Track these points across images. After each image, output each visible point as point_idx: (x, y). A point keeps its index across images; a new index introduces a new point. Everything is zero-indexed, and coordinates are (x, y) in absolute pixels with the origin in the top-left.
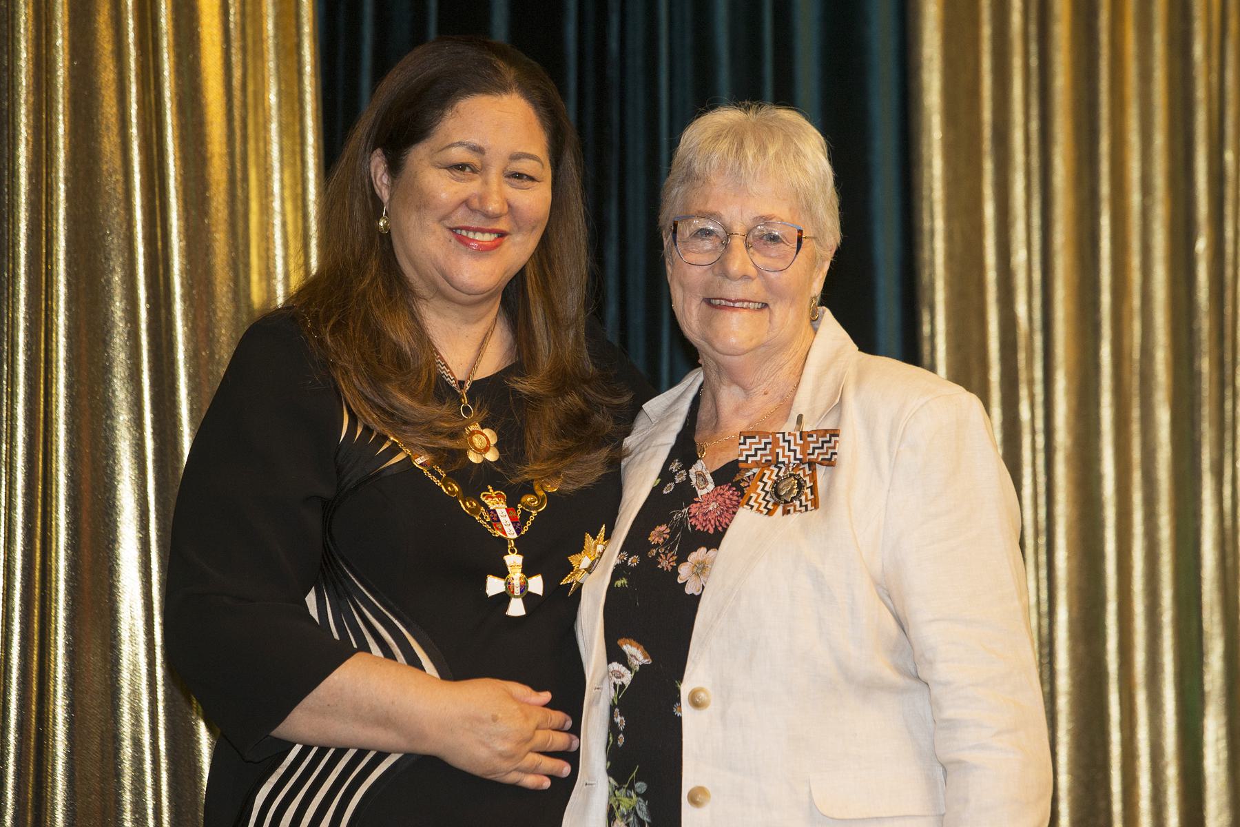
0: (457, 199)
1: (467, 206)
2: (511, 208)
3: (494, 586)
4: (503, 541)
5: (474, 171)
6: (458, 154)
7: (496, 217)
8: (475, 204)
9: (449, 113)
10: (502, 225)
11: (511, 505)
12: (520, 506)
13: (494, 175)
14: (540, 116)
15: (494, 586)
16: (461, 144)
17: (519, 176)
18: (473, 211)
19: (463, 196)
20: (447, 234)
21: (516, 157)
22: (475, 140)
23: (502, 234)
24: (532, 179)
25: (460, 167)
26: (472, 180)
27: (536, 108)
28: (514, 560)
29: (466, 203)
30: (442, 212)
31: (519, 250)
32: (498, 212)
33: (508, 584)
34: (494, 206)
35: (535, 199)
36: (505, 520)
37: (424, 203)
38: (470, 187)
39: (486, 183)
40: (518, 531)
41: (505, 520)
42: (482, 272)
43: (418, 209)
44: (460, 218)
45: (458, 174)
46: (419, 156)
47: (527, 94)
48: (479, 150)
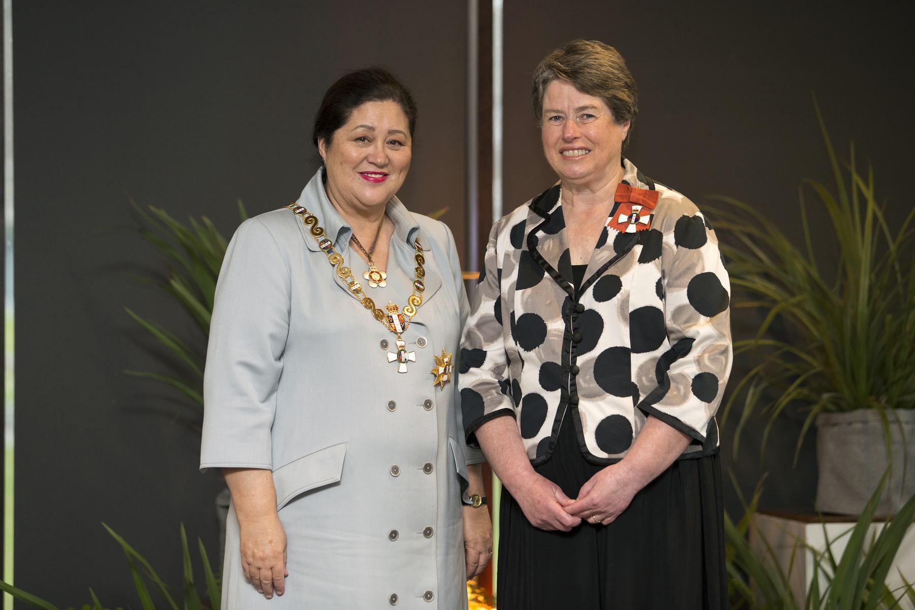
0: (362, 156)
6: (360, 132)
10: (385, 170)
13: (379, 143)
16: (362, 126)
17: (393, 142)
21: (391, 132)
22: (368, 123)
23: (385, 175)
24: (401, 144)
25: (362, 139)
26: (369, 146)
29: (366, 158)
34: (380, 160)
35: (402, 155)
38: (370, 150)
45: (360, 143)
46: (341, 135)
48: (372, 129)
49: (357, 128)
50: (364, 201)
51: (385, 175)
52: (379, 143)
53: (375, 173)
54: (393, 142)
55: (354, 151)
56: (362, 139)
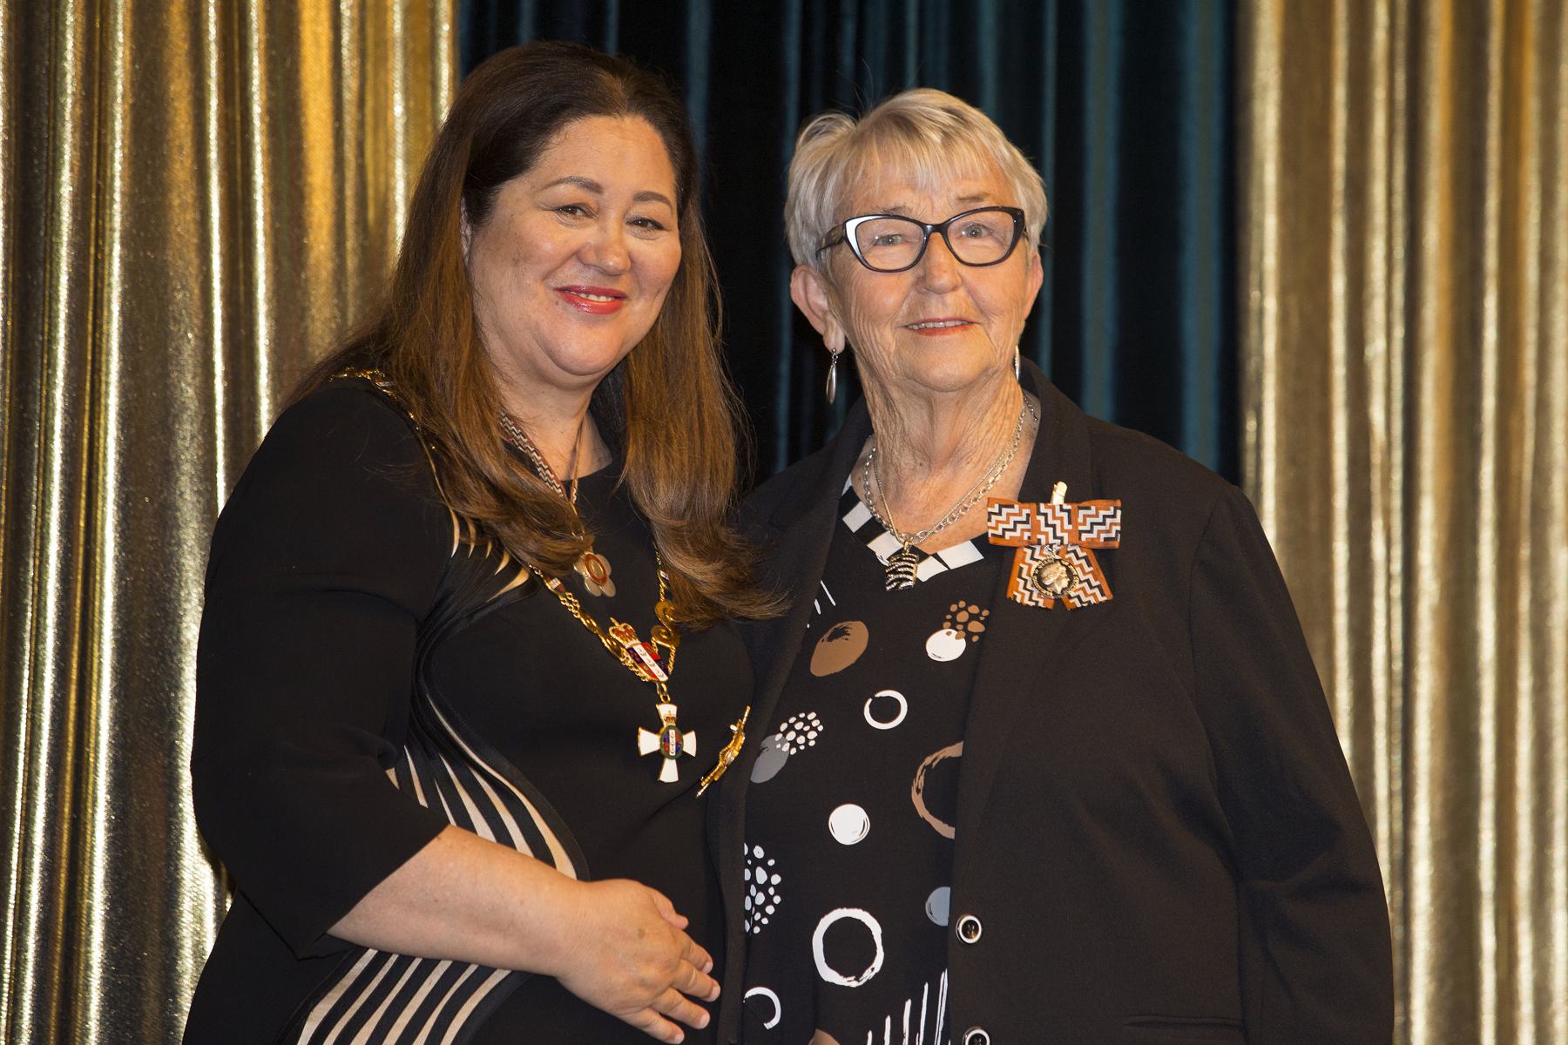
0: (566, 250)
1: (580, 260)
2: (633, 265)
3: (648, 742)
4: (652, 685)
5: (588, 214)
6: (568, 193)
7: (614, 275)
8: (591, 258)
9: (555, 139)
10: (621, 286)
11: (646, 641)
12: (654, 641)
13: (613, 218)
14: (669, 146)
15: (648, 742)
16: (570, 180)
17: (642, 222)
18: (587, 265)
19: (574, 245)
20: (553, 295)
21: (643, 197)
22: (590, 174)
23: (620, 297)
24: (658, 227)
25: (570, 209)
26: (584, 226)
27: (664, 135)
28: (667, 710)
29: (577, 255)
30: (545, 267)
31: (641, 314)
32: (621, 267)
33: (665, 740)
34: (614, 261)
35: (660, 252)
36: (647, 659)
37: (522, 255)
38: (584, 234)
39: (603, 229)
40: (666, 671)
41: (647, 659)
42: (591, 344)
43: (516, 262)
44: (573, 275)
45: (568, 218)
46: (514, 196)
47: (652, 119)
48: (595, 188)
49: (559, 182)
50: (566, 361)
51: (620, 297)
52: (613, 218)
53: (599, 293)
54: (642, 222)
55: (552, 236)
56: (570, 209)
